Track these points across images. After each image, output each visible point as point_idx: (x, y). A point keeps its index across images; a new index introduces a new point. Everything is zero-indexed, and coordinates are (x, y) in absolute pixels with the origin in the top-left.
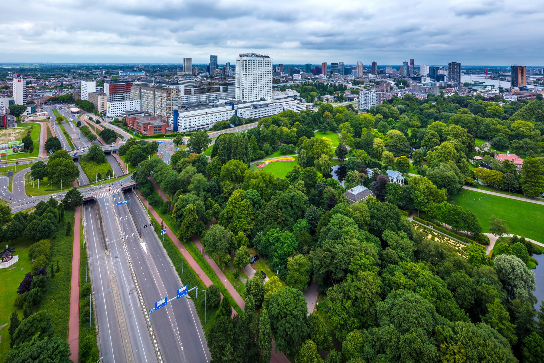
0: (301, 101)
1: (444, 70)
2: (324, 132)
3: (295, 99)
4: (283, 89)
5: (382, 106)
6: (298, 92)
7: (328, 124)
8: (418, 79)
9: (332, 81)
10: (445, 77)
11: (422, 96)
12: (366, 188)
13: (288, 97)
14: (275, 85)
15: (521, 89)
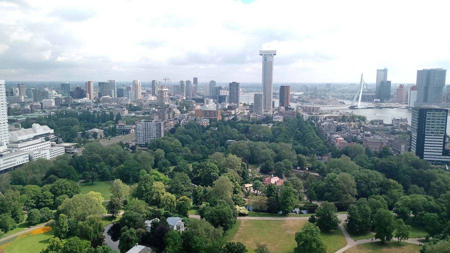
0: (57, 141)
1: (225, 90)
2: (91, 182)
3: (47, 139)
4: (27, 125)
5: (163, 139)
6: (51, 128)
7: (97, 170)
8: (200, 101)
9: (100, 107)
10: (227, 98)
11: (205, 122)
12: (145, 247)
13: (36, 138)
14: (12, 117)
15: (287, 109)
